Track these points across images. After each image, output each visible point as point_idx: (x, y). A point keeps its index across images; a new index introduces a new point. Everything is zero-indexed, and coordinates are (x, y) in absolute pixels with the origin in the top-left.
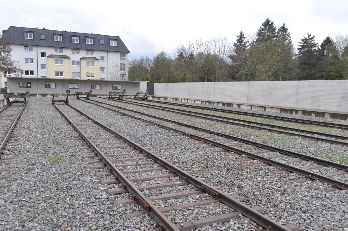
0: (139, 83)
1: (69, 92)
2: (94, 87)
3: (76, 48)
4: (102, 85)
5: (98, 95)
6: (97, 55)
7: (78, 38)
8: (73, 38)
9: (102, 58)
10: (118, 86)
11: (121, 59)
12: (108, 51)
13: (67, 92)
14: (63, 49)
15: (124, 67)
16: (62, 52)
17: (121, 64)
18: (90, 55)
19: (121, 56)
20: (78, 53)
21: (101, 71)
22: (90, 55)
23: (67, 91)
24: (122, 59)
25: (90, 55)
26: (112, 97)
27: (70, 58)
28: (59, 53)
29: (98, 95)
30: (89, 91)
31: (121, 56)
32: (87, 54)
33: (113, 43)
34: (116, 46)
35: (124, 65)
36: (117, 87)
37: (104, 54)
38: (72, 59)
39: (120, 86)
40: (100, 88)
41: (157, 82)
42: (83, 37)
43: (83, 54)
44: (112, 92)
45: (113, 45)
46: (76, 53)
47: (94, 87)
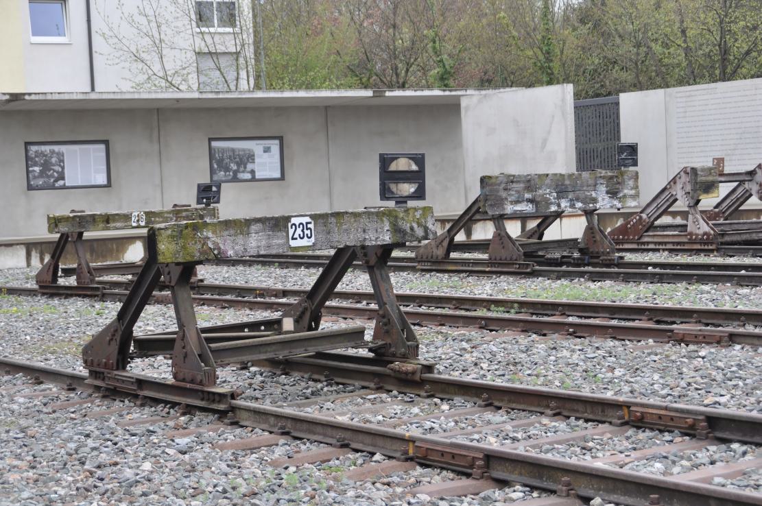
0: (452, 109)
1: (417, 177)
2: (46, 166)
4: (118, 146)
5: (132, 239)
10: (256, 147)
13: (388, 177)
21: (35, 34)
23: (385, 161)
26: (501, 235)
29: (132, 239)
30: (189, 198)
36: (246, 159)
39: (275, 146)
40: (101, 179)
41: (577, 95)
44: (512, 179)
47: (46, 166)
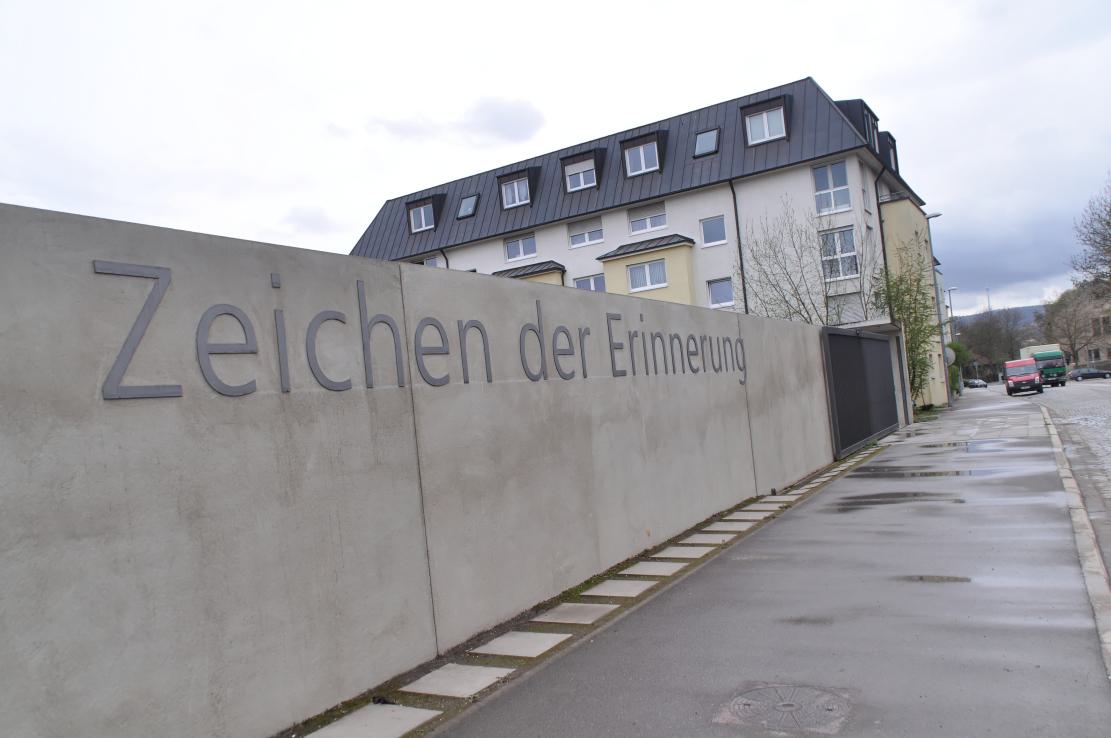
3: (582, 218)
6: (682, 218)
7: (590, 164)
8: (570, 170)
9: (713, 229)
11: (822, 203)
12: (731, 183)
14: (533, 233)
15: (848, 245)
16: (534, 251)
17: (826, 236)
18: (650, 231)
19: (820, 184)
20: (598, 234)
22: (649, 229)
24: (828, 205)
25: (649, 229)
27: (562, 270)
28: (522, 257)
31: (817, 190)
32: (637, 225)
33: (767, 128)
34: (784, 134)
35: (846, 231)
37: (716, 204)
38: (573, 272)
42: (599, 153)
43: (618, 231)
45: (767, 138)
46: (586, 235)
